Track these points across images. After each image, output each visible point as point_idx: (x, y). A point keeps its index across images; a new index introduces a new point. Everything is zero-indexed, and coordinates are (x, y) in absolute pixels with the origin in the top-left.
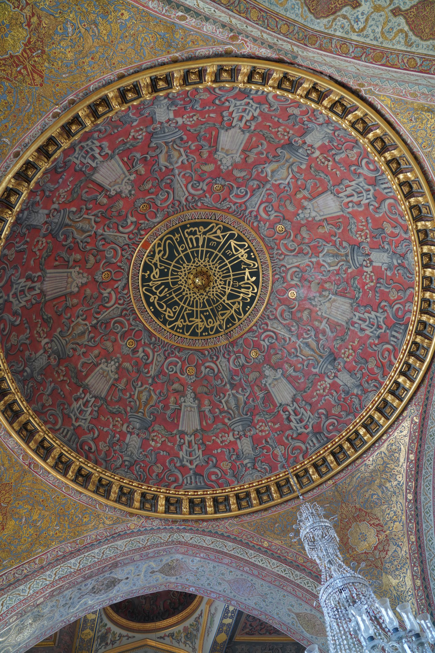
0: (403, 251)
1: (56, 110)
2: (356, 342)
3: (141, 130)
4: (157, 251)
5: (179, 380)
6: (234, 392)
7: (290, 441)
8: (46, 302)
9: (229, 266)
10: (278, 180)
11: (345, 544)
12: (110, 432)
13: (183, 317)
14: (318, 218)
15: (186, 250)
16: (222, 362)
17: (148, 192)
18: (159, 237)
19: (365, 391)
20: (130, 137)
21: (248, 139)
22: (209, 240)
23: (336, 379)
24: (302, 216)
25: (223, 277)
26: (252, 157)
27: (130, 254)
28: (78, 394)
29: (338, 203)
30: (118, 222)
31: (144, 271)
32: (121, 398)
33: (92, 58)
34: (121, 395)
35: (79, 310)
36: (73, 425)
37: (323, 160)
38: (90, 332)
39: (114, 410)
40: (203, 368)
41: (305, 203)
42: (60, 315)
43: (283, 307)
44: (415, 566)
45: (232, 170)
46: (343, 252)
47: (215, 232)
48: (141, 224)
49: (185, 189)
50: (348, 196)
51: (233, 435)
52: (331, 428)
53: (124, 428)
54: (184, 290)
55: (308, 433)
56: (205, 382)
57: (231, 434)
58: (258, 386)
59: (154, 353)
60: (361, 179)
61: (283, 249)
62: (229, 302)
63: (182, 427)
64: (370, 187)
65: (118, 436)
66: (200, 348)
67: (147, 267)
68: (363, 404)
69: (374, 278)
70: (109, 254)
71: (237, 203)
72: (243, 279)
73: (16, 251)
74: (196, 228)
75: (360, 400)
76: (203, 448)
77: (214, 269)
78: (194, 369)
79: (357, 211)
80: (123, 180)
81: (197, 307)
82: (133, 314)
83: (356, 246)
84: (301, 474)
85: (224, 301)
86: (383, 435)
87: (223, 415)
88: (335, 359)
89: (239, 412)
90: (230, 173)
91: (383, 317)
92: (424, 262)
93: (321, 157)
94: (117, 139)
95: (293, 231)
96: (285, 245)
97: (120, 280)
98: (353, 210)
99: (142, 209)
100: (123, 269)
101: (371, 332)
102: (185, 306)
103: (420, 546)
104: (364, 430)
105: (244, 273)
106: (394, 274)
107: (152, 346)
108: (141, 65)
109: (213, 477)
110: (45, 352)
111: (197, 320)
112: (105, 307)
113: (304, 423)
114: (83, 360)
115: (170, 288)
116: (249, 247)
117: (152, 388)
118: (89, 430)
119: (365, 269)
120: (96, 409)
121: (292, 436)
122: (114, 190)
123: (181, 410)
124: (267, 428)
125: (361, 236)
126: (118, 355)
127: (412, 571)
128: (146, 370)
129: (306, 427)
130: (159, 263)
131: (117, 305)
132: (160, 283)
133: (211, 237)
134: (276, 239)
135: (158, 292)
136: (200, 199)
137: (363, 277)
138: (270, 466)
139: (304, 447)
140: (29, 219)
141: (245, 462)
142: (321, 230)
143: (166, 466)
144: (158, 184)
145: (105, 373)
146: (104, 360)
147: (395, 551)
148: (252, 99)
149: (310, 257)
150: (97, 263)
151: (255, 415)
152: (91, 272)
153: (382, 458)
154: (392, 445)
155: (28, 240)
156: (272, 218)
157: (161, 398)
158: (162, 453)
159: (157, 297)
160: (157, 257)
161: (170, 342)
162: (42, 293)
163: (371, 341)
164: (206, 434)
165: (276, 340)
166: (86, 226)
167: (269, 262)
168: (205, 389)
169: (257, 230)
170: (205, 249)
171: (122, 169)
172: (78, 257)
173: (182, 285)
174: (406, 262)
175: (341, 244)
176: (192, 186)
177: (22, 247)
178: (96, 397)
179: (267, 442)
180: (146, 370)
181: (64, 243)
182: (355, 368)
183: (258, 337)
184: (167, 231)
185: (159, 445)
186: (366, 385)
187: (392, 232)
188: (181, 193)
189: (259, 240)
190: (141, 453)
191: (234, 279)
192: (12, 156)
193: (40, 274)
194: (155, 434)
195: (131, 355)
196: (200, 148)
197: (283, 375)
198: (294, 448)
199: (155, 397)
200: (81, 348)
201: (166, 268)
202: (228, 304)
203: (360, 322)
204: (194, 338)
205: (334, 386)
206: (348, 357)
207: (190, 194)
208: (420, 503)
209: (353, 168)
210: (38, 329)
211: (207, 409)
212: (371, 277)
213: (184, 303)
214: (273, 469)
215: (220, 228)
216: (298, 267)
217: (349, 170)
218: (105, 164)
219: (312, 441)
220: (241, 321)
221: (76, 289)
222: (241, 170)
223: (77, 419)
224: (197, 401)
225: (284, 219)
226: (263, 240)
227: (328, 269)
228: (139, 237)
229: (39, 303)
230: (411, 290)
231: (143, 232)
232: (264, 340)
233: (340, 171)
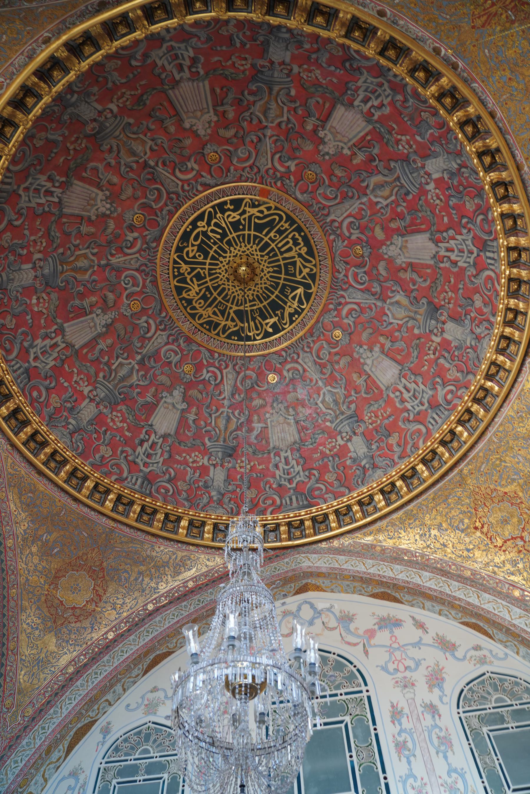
0: (380, 464)
1: (443, 50)
2: (261, 467)
3: (411, 147)
4: (262, 208)
5: (119, 297)
6: (136, 367)
7: (122, 457)
8: (164, 92)
9: (273, 297)
10: (391, 311)
11: (56, 577)
12: (26, 240)
13: (193, 269)
14: (366, 368)
15: (273, 241)
16: (161, 338)
17: (330, 174)
18: (279, 205)
19: (220, 503)
20: (399, 137)
21: (426, 265)
22: (294, 264)
23: (212, 468)
24: (361, 351)
25: (257, 296)
26: (407, 275)
27: (248, 178)
28: (58, 178)
29: (392, 381)
30: (285, 150)
31: (232, 202)
32: (69, 235)
33: (510, 79)
34: (73, 234)
35: (162, 139)
36: (19, 186)
37: (432, 348)
38: (137, 162)
39: (53, 233)
40: (144, 318)
41: (377, 349)
42: (150, 116)
43: (254, 375)
44: (85, 655)
45: (384, 259)
46: (344, 408)
47: (305, 267)
48: (289, 179)
49: (345, 215)
50: (405, 388)
51: (90, 391)
52: (163, 491)
53: (37, 256)
54: (225, 257)
55: (141, 471)
56: (130, 329)
57: (90, 388)
58: (156, 390)
59: (138, 252)
60: (431, 393)
61: (316, 347)
62: (232, 314)
63: (69, 327)
64: (427, 405)
65: (25, 252)
66: (166, 304)
67: (237, 204)
68: (207, 508)
69: (335, 450)
70: (242, 153)
71: (348, 278)
72: (264, 318)
73: (233, 34)
74: (302, 244)
75: (209, 503)
76: (58, 363)
77: (263, 282)
78: (139, 309)
79: (394, 403)
80: (340, 141)
81: (211, 280)
82: (175, 207)
83: (357, 417)
84: (101, 489)
85: (231, 308)
86: (193, 545)
87: (106, 368)
88: (230, 456)
89: (117, 384)
90: (380, 258)
91: (302, 479)
92: (385, 489)
93: (434, 345)
94: (394, 123)
95: (341, 348)
96: (321, 347)
97: (212, 176)
98: (392, 399)
99: (309, 174)
100: (227, 175)
101: (280, 476)
102: (207, 267)
103: (108, 647)
104: (187, 525)
105: (271, 317)
106: (351, 468)
107: (145, 246)
108: (509, 134)
109: (35, 394)
110: (100, 113)
111: (196, 287)
112: (174, 170)
113: (148, 460)
114: (101, 166)
115: (221, 240)
116: (303, 310)
117: (95, 269)
118: (19, 211)
119: (339, 438)
120: (47, 209)
121: (127, 456)
122: (326, 134)
123: (87, 315)
124: (118, 424)
125: (370, 418)
126: (119, 209)
127: (78, 656)
128: (114, 252)
129: (146, 465)
130: (246, 216)
131: (180, 183)
132: (224, 225)
133: (298, 264)
134: (324, 335)
135: (213, 227)
136: (338, 235)
137: (330, 440)
138: (84, 450)
139: (125, 475)
140: (278, 41)
141: (71, 420)
142: (355, 376)
143: (17, 331)
144: (344, 183)
145: (92, 202)
146: (108, 193)
147: (85, 628)
148: (478, 255)
149: (321, 379)
150: (227, 141)
151: (125, 404)
152: (215, 138)
153: (170, 558)
154: (190, 559)
155: (248, 46)
156: (346, 321)
157: (89, 286)
158: (28, 317)
159: (204, 229)
160: (254, 211)
161: (158, 266)
162: (175, 83)
163: (272, 480)
164: (74, 359)
165: (216, 385)
166: (272, 114)
167: (296, 338)
168: (122, 333)
169: (325, 310)
170: (282, 263)
171: (354, 137)
172: (231, 115)
173: (231, 252)
174: (370, 472)
175: (351, 402)
176: (351, 222)
177: (238, 41)
178: (60, 202)
179: (106, 432)
180: (114, 252)
181: (246, 92)
182: (235, 479)
183: (210, 365)
184: (289, 212)
185: (36, 309)
186: (226, 500)
187: (392, 445)
188: (339, 212)
189: (316, 317)
190: (17, 292)
191: (260, 309)
192: (379, 8)
193: (202, 72)
194: (46, 298)
195: (125, 225)
196: (401, 216)
197: (183, 411)
198: (118, 466)
199: (87, 277)
200: (115, 159)
201: (244, 226)
202: (229, 313)
203: (283, 460)
204: (174, 293)
205: (204, 470)
206: (241, 467)
207: (341, 223)
208: (151, 620)
209: (438, 380)
210: (128, 93)
211: (102, 345)
212: (335, 447)
213: (210, 264)
214: (83, 455)
215: (312, 270)
216: (305, 370)
217: (434, 377)
218: (359, 116)
219: (137, 479)
220: (216, 337)
221: (187, 125)
222: (387, 269)
223: (27, 189)
224: (104, 329)
225: (350, 334)
226: (318, 321)
227: (318, 402)
228: (273, 181)
229: (162, 84)
230: (347, 491)
231: (279, 184)
232: (208, 372)
233: (429, 369)
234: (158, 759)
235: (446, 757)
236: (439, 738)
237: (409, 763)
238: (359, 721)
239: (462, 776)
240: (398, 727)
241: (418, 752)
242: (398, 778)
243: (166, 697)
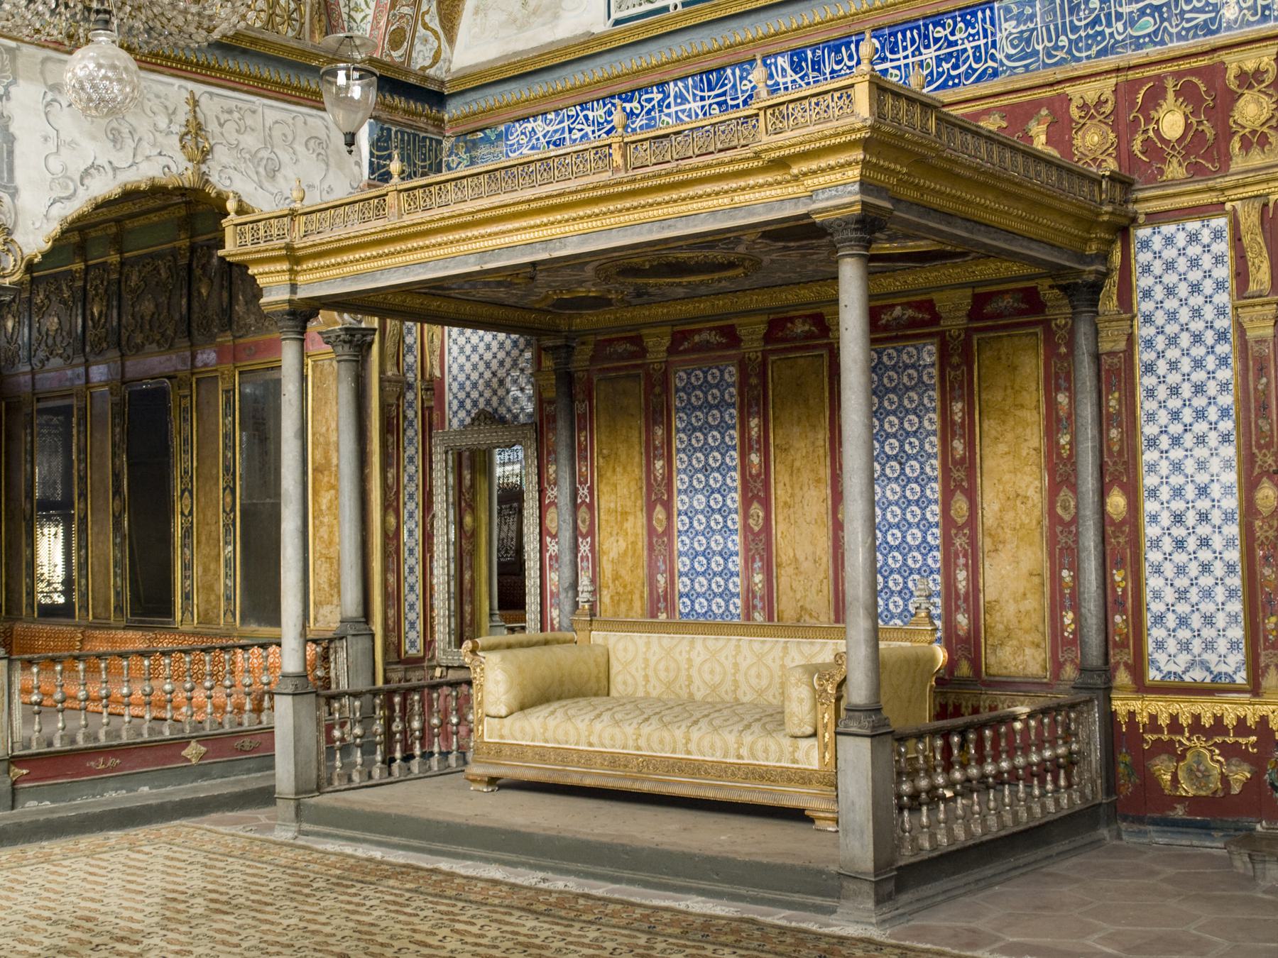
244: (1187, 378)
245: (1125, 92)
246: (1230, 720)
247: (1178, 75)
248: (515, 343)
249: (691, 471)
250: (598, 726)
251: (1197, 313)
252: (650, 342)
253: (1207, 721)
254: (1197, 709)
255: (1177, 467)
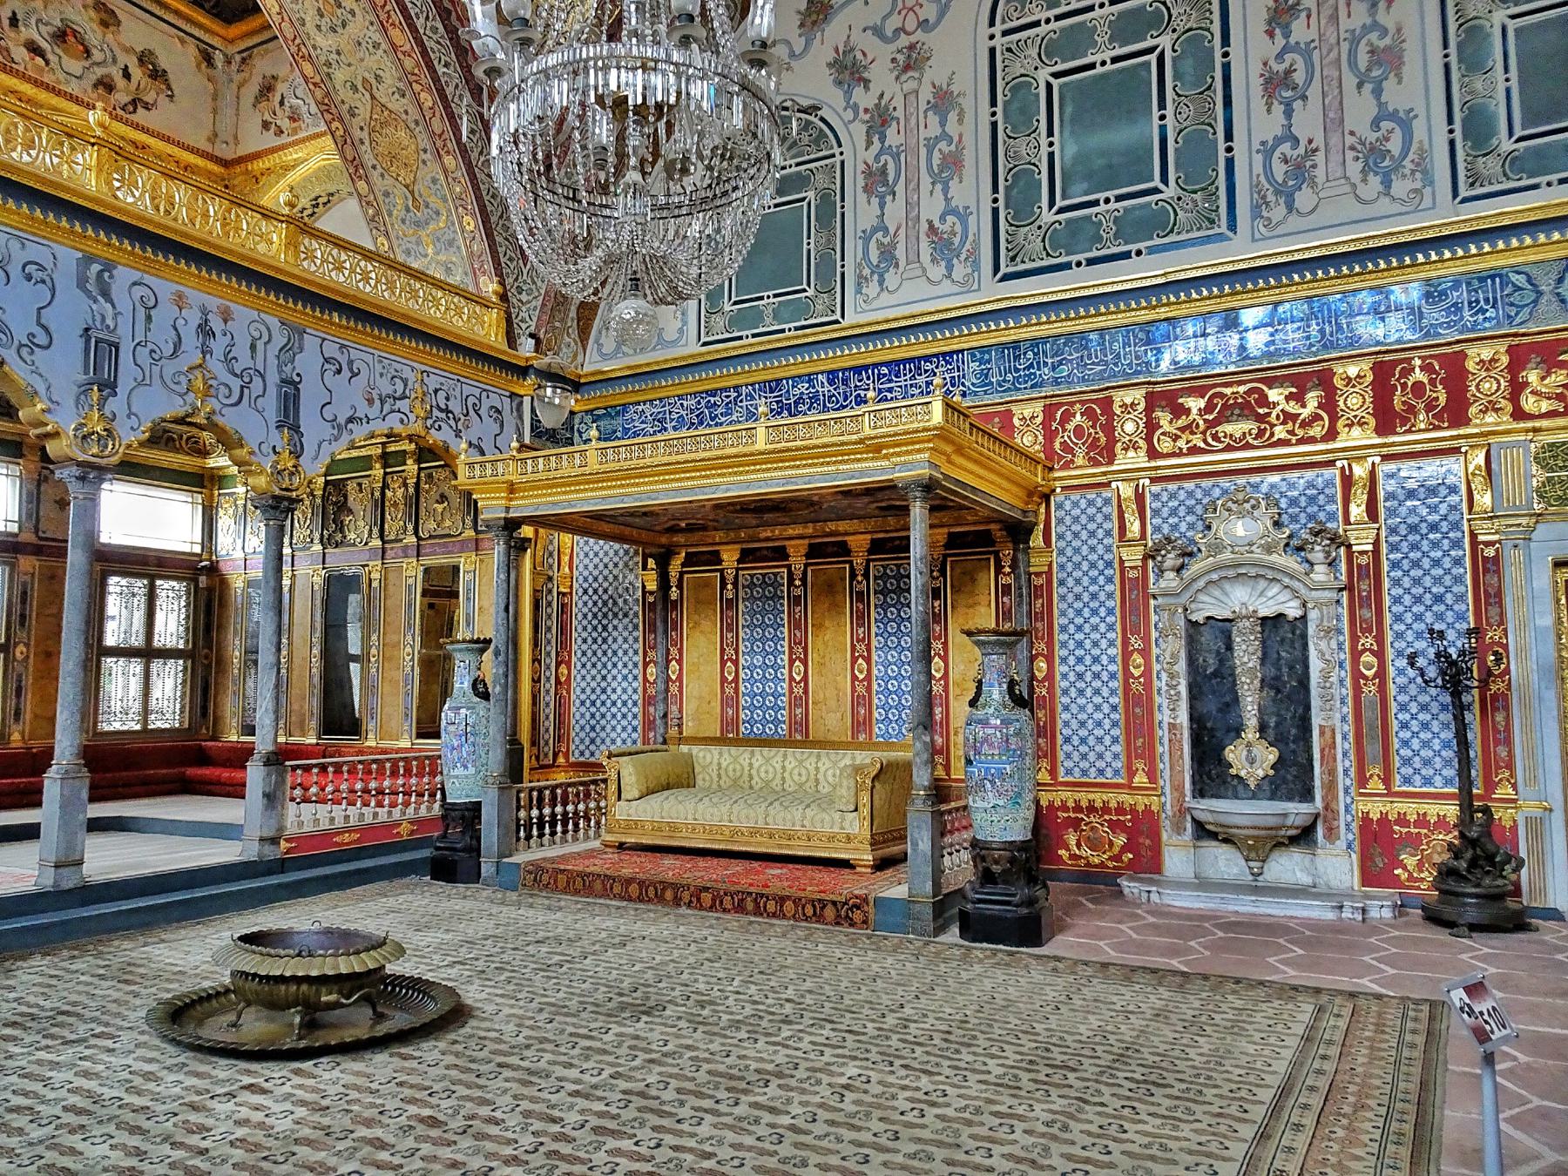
234: (794, 169)
235: (1378, 92)
236: (1372, 52)
237: (1289, 113)
238: (1194, 43)
239: (1406, 124)
240: (1280, 41)
241: (1314, 92)
242: (1256, 146)
243: (792, 55)
244: (1086, 589)
245: (1049, 411)
246: (1113, 804)
247: (1083, 402)
248: (626, 552)
249: (753, 641)
250: (701, 806)
251: (1093, 549)
252: (725, 557)
253: (1099, 804)
254: (1091, 796)
255: (1080, 644)
